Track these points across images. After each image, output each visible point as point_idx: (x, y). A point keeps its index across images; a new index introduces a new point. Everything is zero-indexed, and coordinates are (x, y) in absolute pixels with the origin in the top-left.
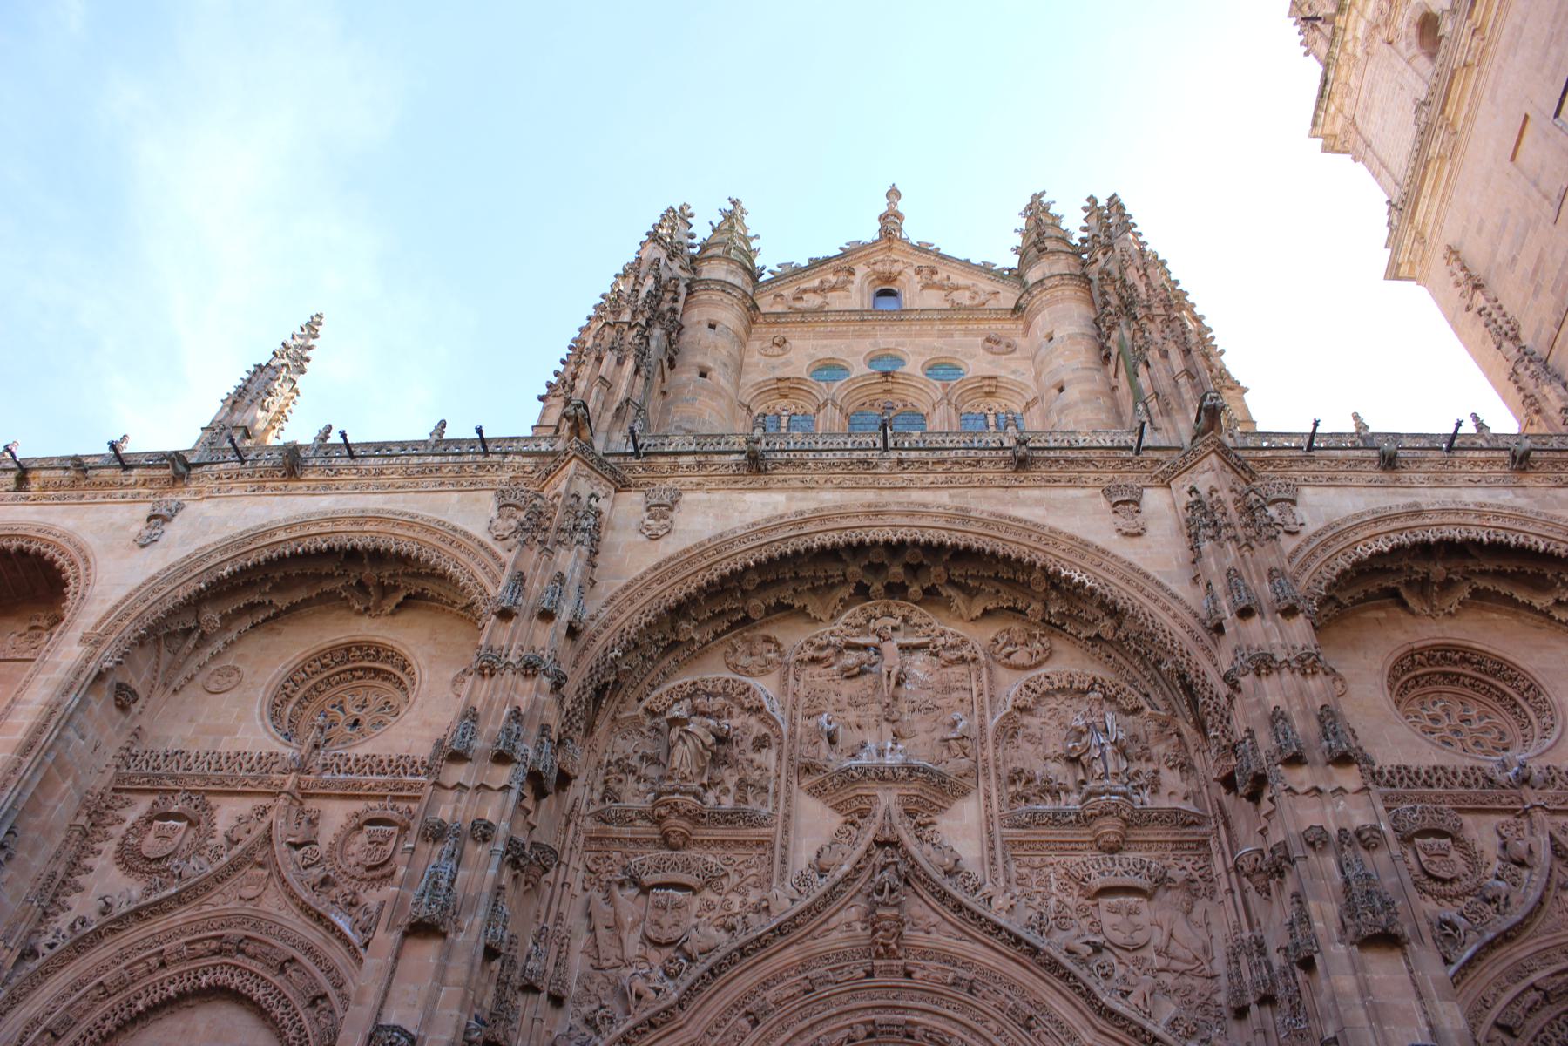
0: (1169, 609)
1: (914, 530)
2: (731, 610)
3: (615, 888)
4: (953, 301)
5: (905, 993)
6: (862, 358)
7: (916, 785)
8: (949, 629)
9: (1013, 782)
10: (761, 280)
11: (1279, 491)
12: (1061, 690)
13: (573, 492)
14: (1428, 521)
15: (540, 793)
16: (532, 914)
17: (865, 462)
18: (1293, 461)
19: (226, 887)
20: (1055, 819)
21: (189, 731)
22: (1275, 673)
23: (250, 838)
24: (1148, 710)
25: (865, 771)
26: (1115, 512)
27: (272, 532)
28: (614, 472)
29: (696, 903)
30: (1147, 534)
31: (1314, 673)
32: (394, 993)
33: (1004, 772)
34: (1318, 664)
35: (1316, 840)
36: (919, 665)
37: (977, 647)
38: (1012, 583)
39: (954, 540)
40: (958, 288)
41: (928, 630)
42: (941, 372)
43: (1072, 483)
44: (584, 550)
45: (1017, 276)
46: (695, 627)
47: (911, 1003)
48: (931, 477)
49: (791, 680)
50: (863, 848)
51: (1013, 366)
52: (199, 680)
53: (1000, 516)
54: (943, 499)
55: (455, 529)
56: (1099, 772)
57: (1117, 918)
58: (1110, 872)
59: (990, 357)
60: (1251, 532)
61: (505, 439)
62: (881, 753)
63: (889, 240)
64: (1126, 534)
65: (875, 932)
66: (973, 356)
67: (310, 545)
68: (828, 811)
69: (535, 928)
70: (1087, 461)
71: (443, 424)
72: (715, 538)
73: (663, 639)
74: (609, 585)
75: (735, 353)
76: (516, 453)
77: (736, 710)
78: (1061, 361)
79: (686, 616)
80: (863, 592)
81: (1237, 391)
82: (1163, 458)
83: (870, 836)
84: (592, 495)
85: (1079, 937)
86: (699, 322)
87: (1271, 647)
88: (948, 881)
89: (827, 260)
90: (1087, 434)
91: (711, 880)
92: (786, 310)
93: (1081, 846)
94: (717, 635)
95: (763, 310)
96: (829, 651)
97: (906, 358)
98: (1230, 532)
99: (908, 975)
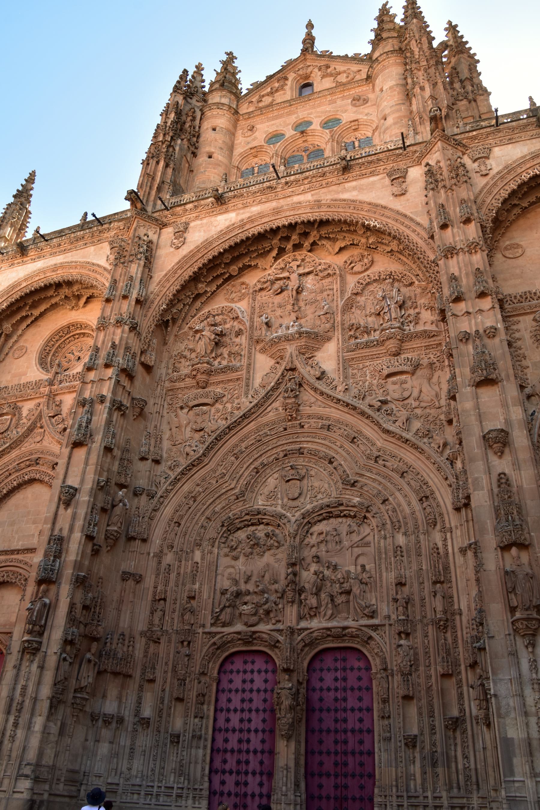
0: (416, 231)
1: (296, 216)
2: (221, 274)
3: (179, 410)
4: (337, 82)
5: (301, 435)
6: (290, 126)
7: (304, 340)
8: (322, 261)
9: (350, 330)
11: (479, 153)
12: (375, 281)
13: (137, 235)
15: (131, 377)
16: (142, 427)
17: (270, 187)
18: (488, 134)
19: (30, 439)
20: (367, 345)
21: (9, 377)
22: (455, 257)
23: (33, 418)
24: (417, 282)
25: (279, 338)
26: (392, 185)
27: (19, 284)
28: (157, 220)
29: (213, 410)
30: (408, 194)
31: (476, 252)
32: (70, 472)
33: (346, 326)
34: (479, 247)
35: (466, 338)
36: (310, 282)
37: (336, 267)
38: (349, 231)
39: (315, 218)
40: (339, 73)
41: (313, 264)
42: (330, 124)
43: (372, 174)
44: (142, 263)
45: (369, 58)
46: (206, 286)
47: (303, 439)
48: (302, 188)
49: (251, 300)
50: (280, 373)
51: (366, 111)
52: (10, 354)
53: (336, 200)
54: (308, 197)
55: (93, 264)
56: (387, 318)
57: (396, 387)
58: (392, 366)
59: (355, 109)
60: (454, 181)
61: (111, 215)
62: (288, 328)
63: (304, 55)
64: (396, 196)
65: (286, 410)
66: (346, 111)
67: (36, 286)
68: (269, 359)
69: (145, 433)
71: (86, 214)
72: (204, 242)
73: (192, 294)
74: (158, 275)
75: (227, 140)
76: (115, 221)
77: (228, 320)
78: (385, 103)
79: (201, 282)
80: (282, 252)
81: (486, 95)
82: (418, 149)
83: (283, 368)
84: (145, 235)
85: (374, 399)
87: (455, 242)
88: (318, 382)
89: (274, 75)
91: (218, 399)
92: (254, 109)
93: (381, 355)
94: (218, 287)
95: (241, 113)
96: (269, 283)
97: (312, 120)
98: (443, 183)
99: (302, 427)
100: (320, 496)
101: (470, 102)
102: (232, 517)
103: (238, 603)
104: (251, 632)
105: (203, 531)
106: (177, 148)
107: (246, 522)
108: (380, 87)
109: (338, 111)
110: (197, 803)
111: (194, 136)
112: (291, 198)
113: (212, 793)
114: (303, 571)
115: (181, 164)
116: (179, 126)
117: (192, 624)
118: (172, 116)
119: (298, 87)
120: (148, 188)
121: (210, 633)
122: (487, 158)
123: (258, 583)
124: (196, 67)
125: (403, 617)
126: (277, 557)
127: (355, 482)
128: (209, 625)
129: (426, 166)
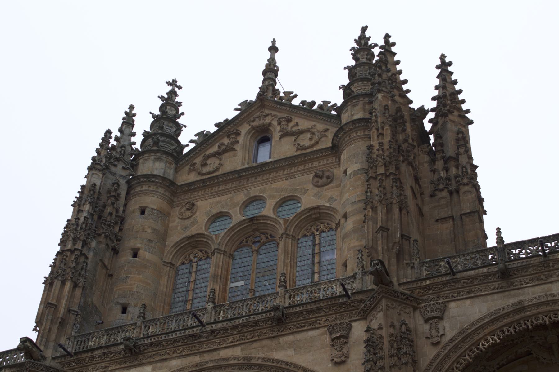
4: (299, 144)
6: (238, 208)
10: (186, 151)
11: (432, 311)
14: (528, 313)
17: (193, 336)
18: (444, 284)
26: (333, 346)
30: (349, 360)
40: (301, 132)
53: (268, 360)
60: (393, 361)
70: (320, 309)
78: (346, 196)
82: (364, 298)
86: (134, 211)
90: (326, 283)
101: (451, 193)
106: (90, 255)
108: (345, 168)
109: (296, 190)
111: (116, 223)
112: (217, 352)
115: (94, 275)
116: (96, 217)
118: (87, 207)
119: (255, 143)
120: (49, 324)
122: (441, 318)
124: (126, 113)
129: (366, 331)
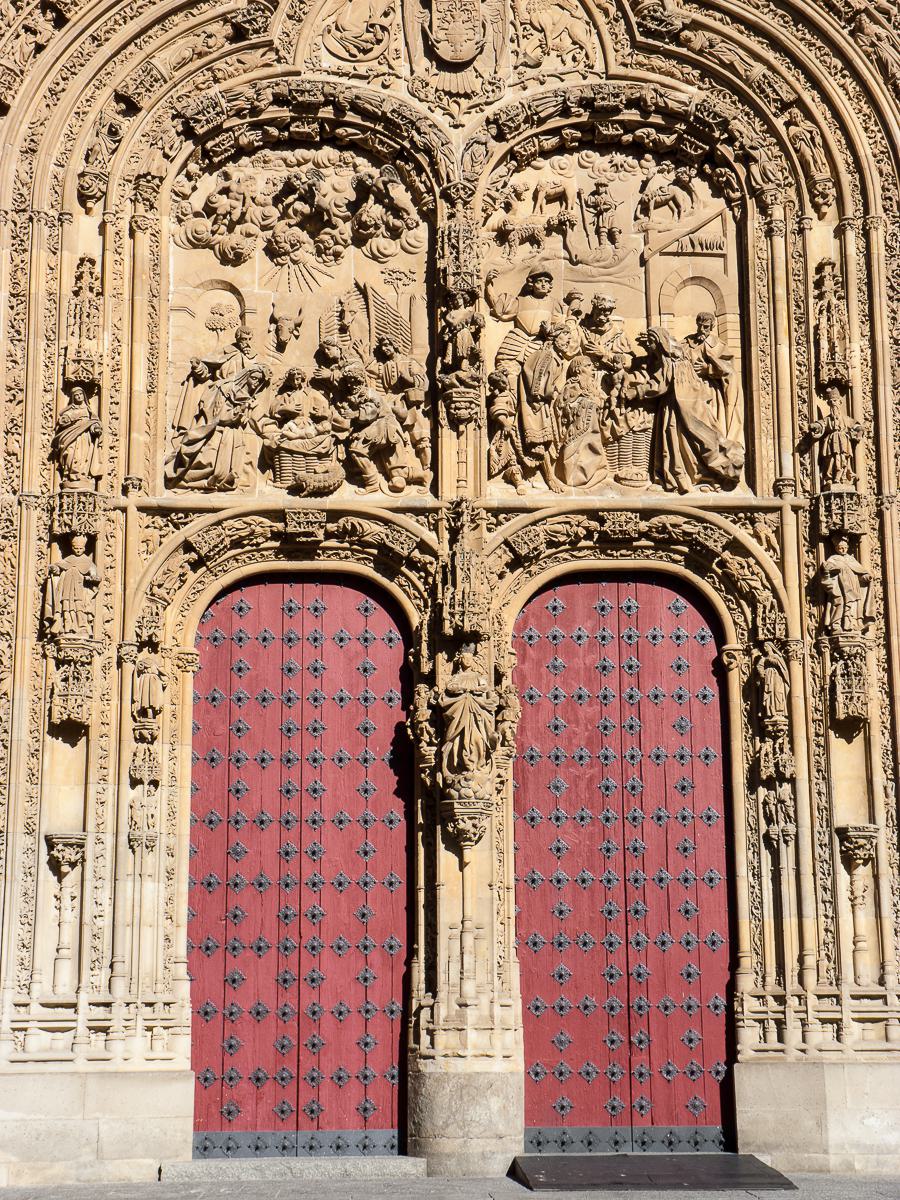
100: (551, 64)
102: (223, 101)
103: (257, 414)
104: (323, 511)
105: (106, 143)
107: (274, 131)
110: (158, 1045)
113: (202, 1013)
114: (490, 321)
117: (98, 478)
121: (163, 511)
123: (334, 352)
125: (848, 487)
126: (392, 264)
127: (685, 27)
128: (160, 482)
